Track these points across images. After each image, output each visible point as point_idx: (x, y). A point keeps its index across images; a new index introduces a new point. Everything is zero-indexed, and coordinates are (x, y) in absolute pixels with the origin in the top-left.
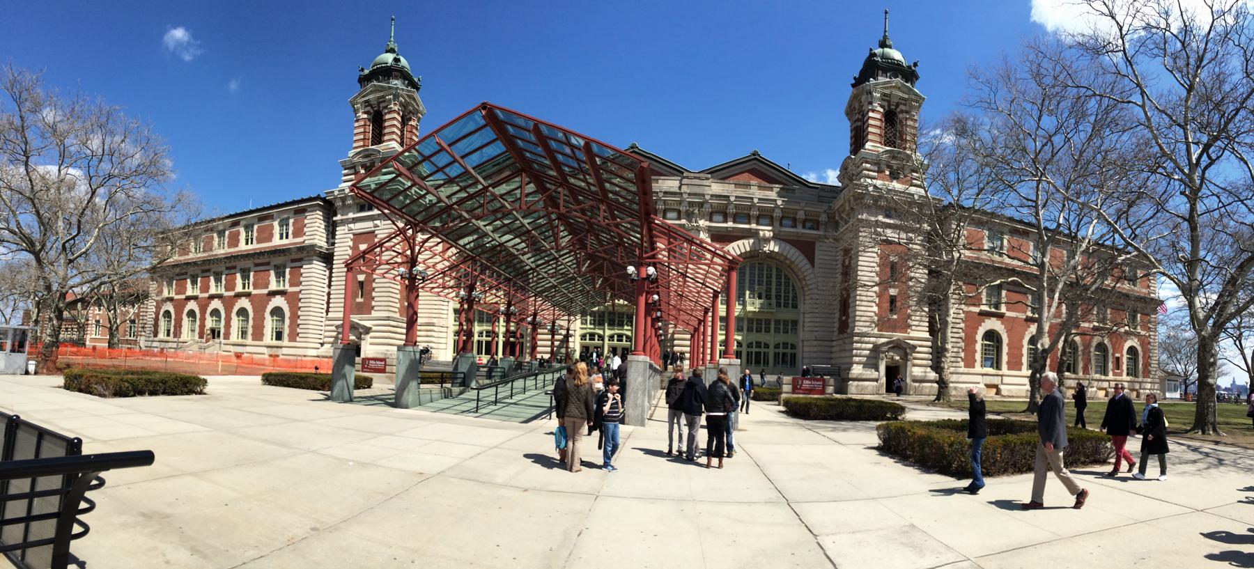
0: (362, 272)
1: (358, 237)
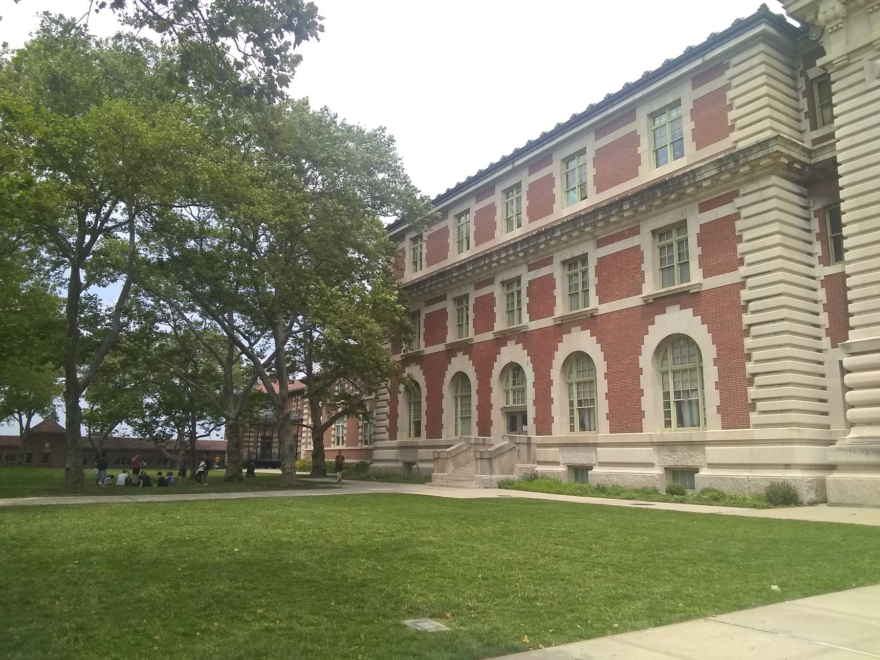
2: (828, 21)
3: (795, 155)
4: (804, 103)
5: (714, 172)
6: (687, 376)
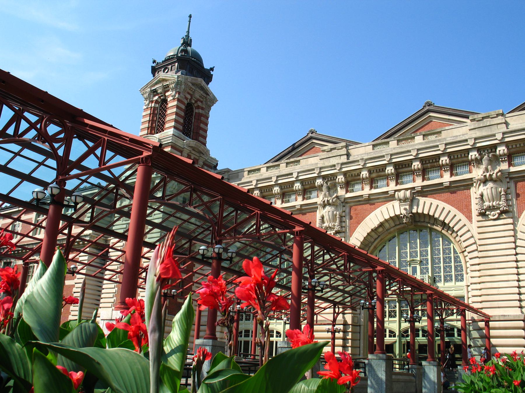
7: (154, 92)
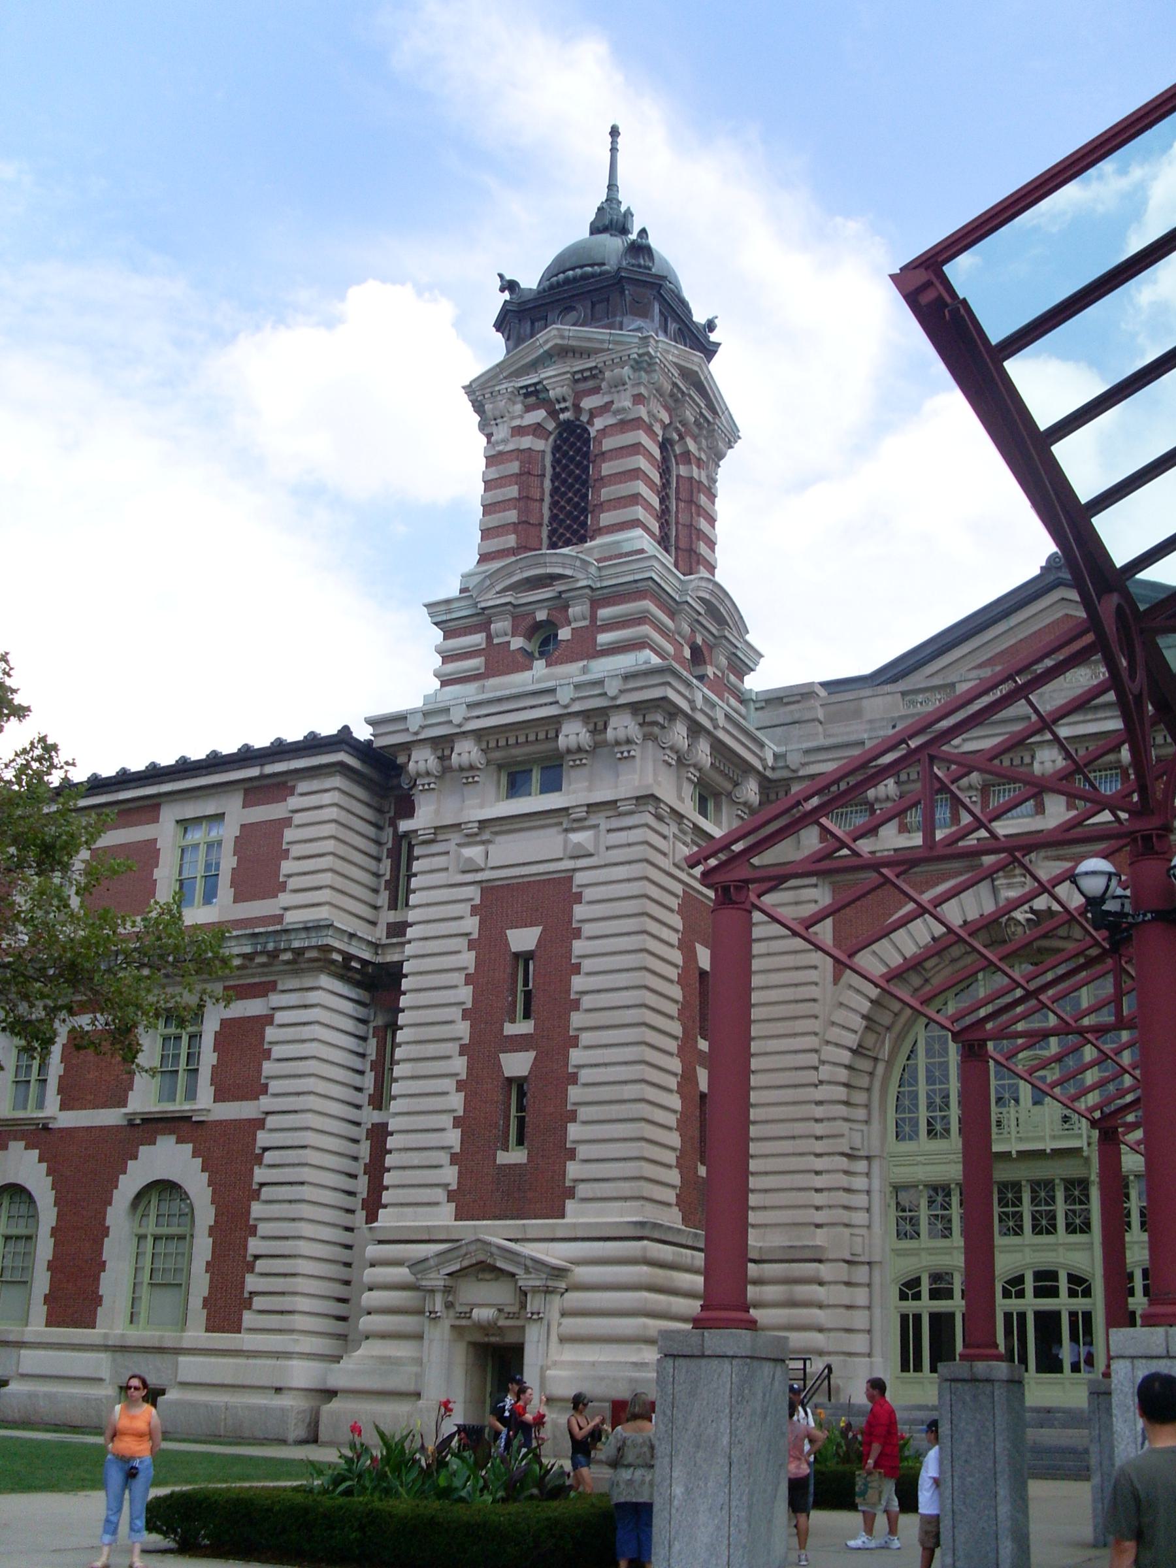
0: (519, 1043)
1: (500, 901)
2: (419, 775)
3: (353, 950)
4: (386, 866)
5: (248, 950)
6: (172, 1247)
7: (526, 395)
